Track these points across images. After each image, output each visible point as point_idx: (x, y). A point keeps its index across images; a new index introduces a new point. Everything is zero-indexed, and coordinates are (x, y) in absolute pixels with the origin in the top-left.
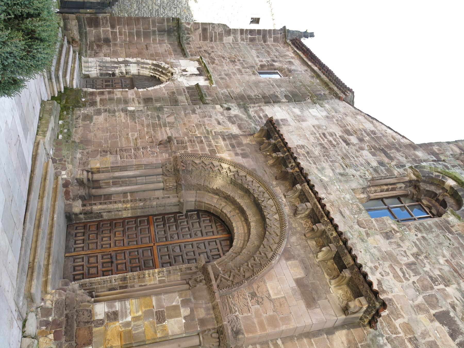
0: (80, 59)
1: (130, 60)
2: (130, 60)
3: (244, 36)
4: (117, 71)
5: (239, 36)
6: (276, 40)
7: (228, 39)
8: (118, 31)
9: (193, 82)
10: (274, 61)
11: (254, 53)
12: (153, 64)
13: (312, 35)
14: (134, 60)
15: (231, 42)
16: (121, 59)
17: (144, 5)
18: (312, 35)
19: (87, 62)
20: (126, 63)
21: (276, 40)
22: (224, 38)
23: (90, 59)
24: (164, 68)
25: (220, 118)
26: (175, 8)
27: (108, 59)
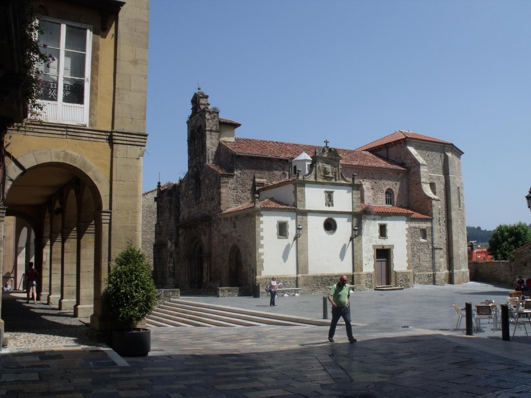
0: (168, 284)
1: (168, 266)
2: (168, 266)
3: (160, 216)
4: (172, 271)
5: (160, 218)
6: (161, 201)
7: (161, 223)
8: (159, 270)
9: (173, 245)
10: (168, 207)
11: (166, 214)
12: (169, 257)
13: (159, 183)
14: (168, 265)
15: (162, 222)
16: (168, 269)
17: (150, 256)
18: (159, 183)
19: (169, 282)
20: (169, 267)
21: (161, 201)
22: (161, 225)
23: (168, 280)
24: (170, 254)
25: (182, 239)
26: (151, 241)
27: (168, 274)
